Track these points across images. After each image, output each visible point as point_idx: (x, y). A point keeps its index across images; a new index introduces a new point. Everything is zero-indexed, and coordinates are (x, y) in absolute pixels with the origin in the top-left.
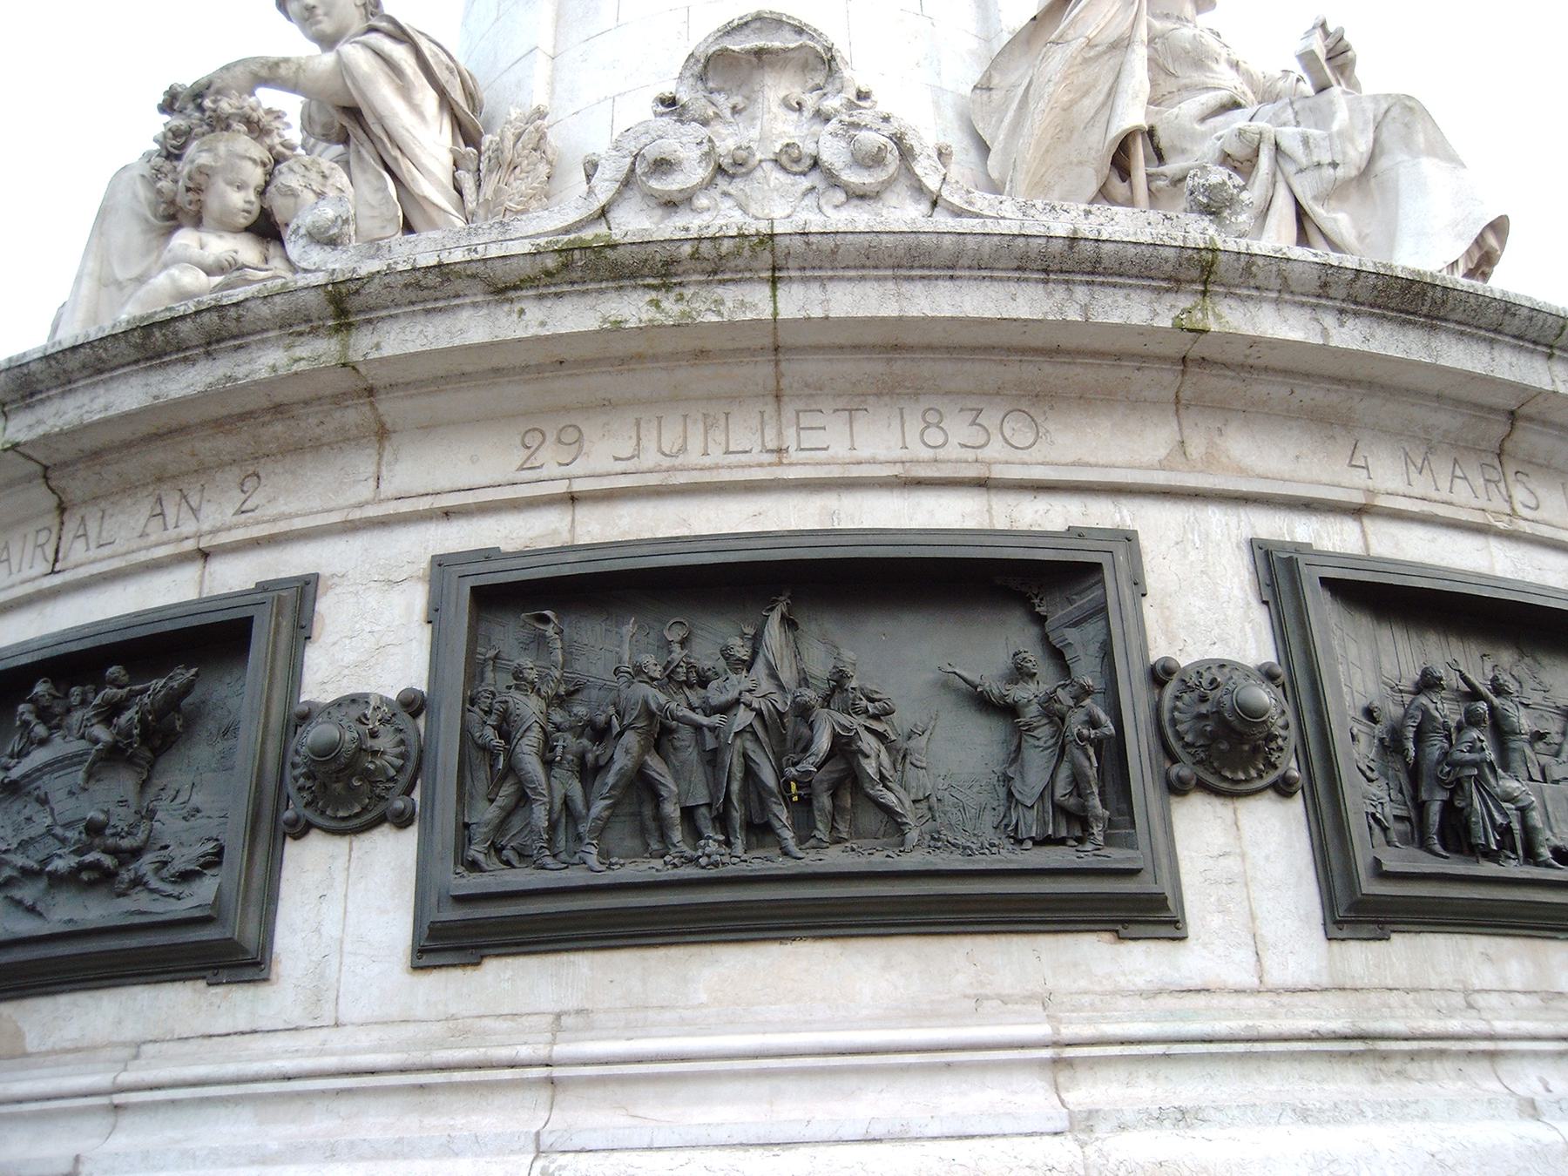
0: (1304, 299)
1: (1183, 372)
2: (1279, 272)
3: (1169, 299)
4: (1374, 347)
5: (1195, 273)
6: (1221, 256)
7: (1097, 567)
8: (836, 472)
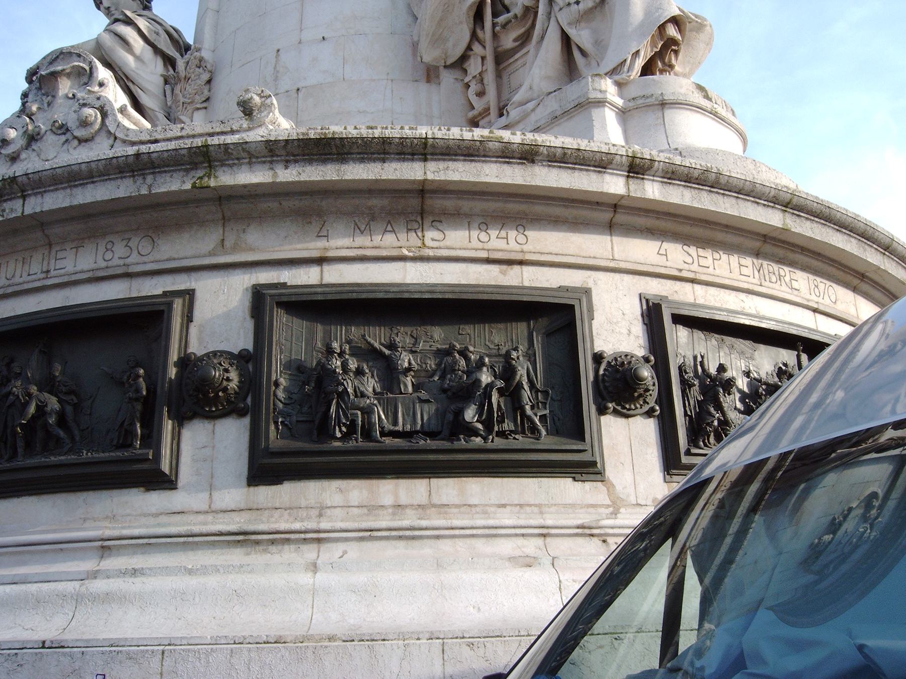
0: (263, 159)
1: (220, 205)
2: (244, 150)
3: (193, 173)
4: (304, 177)
5: (201, 159)
6: (211, 148)
7: (163, 311)
8: (66, 279)
